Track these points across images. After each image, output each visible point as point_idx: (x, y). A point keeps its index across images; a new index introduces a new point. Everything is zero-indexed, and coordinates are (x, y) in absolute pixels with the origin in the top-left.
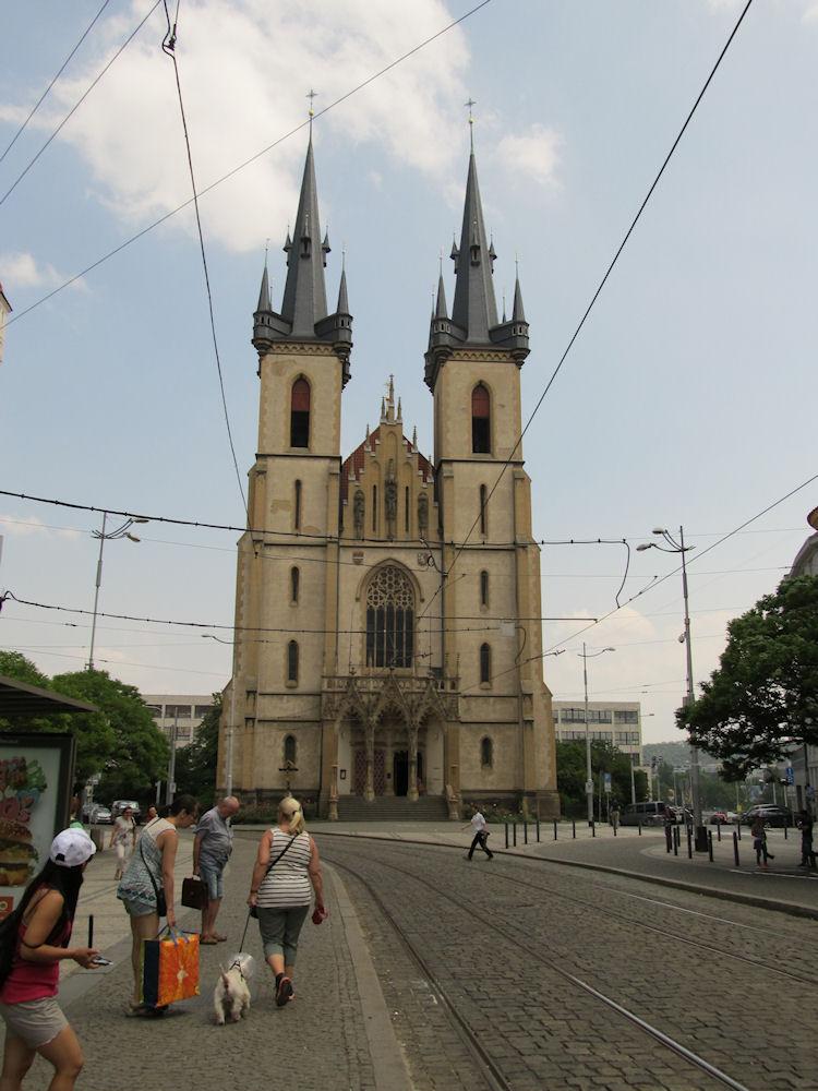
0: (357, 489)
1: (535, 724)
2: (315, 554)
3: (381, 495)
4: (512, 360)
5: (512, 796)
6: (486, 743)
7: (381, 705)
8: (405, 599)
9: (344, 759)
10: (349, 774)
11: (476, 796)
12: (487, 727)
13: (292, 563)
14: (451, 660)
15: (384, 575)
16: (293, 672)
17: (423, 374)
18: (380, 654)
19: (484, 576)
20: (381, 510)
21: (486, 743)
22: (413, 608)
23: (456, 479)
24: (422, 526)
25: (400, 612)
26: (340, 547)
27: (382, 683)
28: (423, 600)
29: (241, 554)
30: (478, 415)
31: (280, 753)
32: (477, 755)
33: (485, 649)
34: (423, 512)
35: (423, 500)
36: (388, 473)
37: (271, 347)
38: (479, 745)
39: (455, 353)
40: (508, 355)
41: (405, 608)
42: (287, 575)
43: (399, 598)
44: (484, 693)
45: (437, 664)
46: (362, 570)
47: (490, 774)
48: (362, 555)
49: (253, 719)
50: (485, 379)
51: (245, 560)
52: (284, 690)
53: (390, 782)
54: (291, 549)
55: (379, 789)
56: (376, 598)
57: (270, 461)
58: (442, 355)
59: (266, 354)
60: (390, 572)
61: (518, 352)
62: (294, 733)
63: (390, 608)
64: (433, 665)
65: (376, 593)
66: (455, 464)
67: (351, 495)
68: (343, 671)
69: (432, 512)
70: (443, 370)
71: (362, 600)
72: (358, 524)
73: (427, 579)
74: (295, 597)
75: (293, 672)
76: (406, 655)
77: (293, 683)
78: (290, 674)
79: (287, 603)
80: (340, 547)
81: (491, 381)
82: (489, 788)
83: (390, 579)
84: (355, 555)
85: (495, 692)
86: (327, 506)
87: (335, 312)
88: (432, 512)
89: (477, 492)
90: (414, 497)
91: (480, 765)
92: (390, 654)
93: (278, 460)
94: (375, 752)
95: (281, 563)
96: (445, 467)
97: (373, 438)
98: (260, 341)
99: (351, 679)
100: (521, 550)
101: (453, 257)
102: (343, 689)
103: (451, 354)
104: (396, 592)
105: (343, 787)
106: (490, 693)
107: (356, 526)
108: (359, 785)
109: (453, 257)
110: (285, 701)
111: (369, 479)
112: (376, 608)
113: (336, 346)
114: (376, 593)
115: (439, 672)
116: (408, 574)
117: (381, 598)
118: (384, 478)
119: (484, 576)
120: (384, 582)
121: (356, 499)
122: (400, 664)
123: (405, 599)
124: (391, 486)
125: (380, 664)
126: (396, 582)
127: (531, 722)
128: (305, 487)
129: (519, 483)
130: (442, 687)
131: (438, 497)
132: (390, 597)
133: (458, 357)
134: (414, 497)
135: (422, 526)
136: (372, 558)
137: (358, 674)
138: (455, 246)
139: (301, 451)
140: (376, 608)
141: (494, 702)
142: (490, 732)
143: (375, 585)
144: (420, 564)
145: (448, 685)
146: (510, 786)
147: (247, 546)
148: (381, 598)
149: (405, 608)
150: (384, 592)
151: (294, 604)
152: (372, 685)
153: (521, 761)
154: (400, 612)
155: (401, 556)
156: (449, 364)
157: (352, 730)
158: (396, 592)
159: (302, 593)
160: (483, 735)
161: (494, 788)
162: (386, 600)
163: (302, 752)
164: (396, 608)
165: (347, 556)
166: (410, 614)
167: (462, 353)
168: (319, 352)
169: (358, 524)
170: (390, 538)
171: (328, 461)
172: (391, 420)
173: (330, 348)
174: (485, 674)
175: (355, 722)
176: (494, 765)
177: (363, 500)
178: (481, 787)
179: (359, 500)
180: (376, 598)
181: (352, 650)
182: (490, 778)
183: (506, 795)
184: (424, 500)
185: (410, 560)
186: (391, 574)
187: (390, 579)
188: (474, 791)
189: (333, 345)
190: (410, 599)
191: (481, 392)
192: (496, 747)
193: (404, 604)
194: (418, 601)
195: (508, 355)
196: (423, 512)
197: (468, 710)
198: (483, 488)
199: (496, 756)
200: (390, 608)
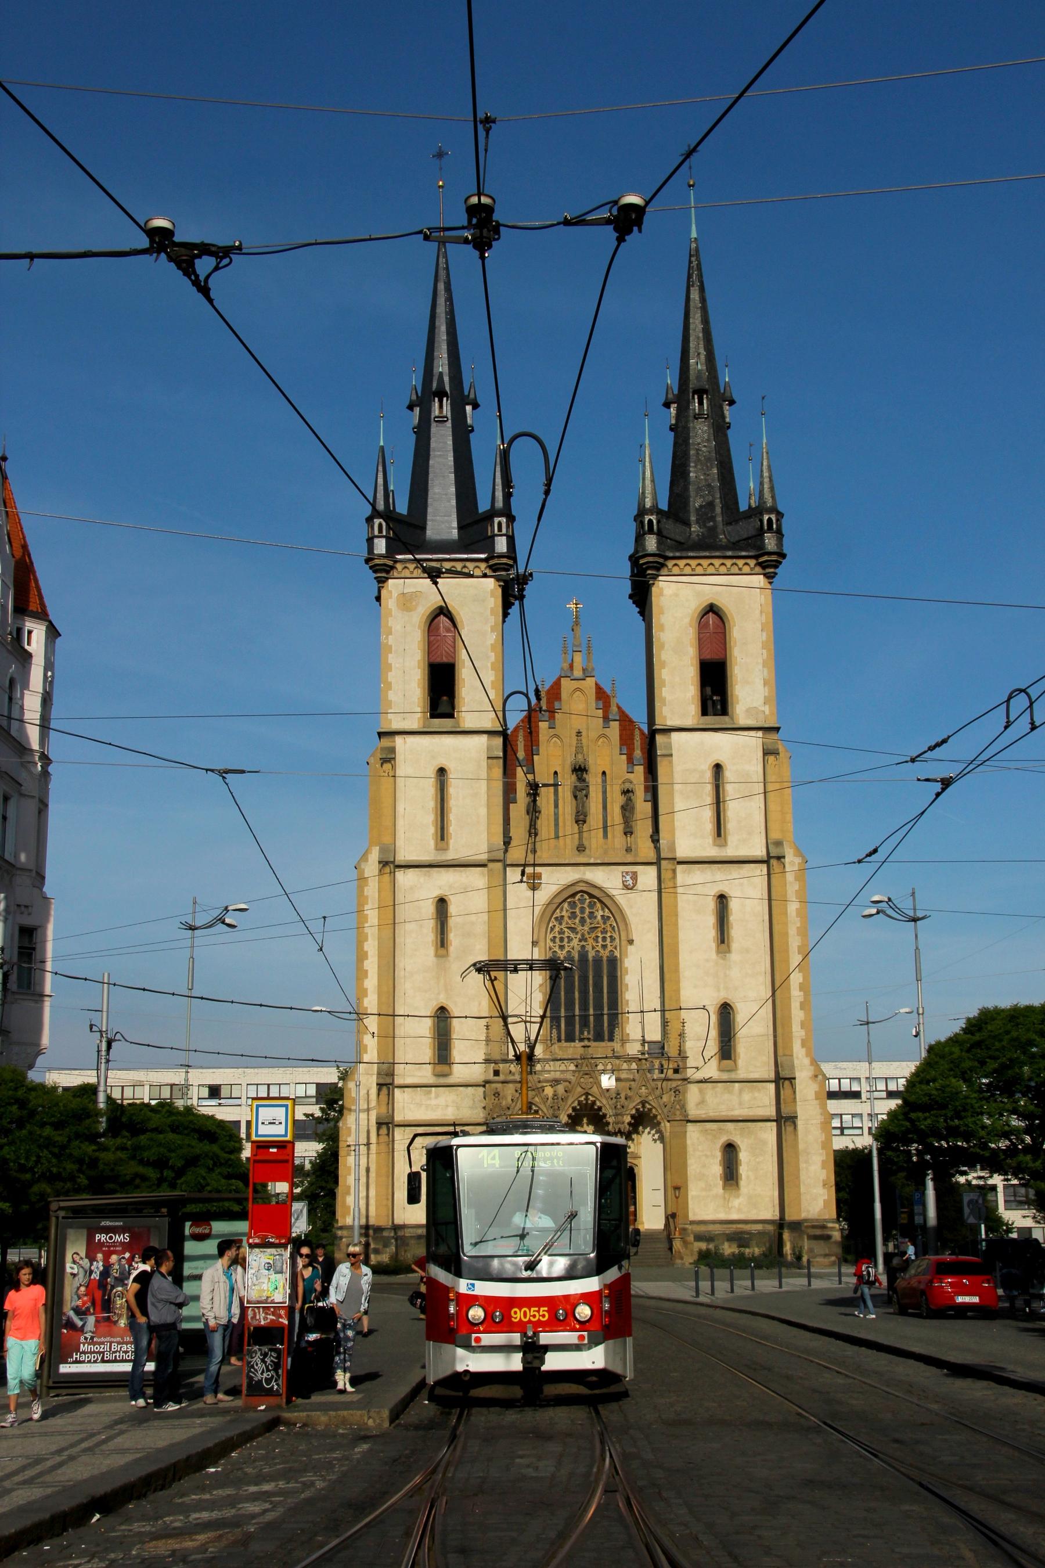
4: (758, 569)
5: (770, 1228)
6: (730, 1150)
8: (604, 939)
11: (717, 1229)
13: (437, 893)
14: (674, 1029)
15: (573, 905)
19: (722, 899)
21: (730, 1150)
22: (617, 953)
23: (674, 757)
25: (598, 961)
26: (506, 866)
27: (572, 1067)
28: (631, 942)
30: (708, 656)
32: (716, 1169)
34: (627, 809)
38: (719, 1155)
39: (670, 563)
41: (605, 954)
43: (596, 939)
44: (725, 1076)
45: (654, 1034)
47: (738, 1196)
50: (715, 602)
52: (432, 1080)
56: (562, 940)
57: (399, 740)
59: (387, 579)
60: (582, 901)
61: (765, 558)
63: (583, 955)
66: (675, 736)
69: (643, 808)
70: (654, 589)
71: (542, 944)
72: (533, 831)
74: (442, 941)
77: (444, 1068)
78: (439, 1056)
79: (431, 951)
80: (506, 866)
82: (734, 1216)
85: (741, 1074)
87: (488, 507)
88: (643, 808)
89: (708, 776)
92: (585, 1023)
93: (411, 739)
96: (660, 739)
98: (377, 562)
102: (517, 1077)
103: (667, 566)
104: (593, 929)
106: (733, 1076)
110: (433, 1095)
114: (561, 932)
117: (570, 939)
118: (570, 760)
120: (573, 915)
122: (599, 1037)
123: (604, 939)
124: (580, 770)
125: (570, 1038)
126: (592, 915)
129: (771, 759)
132: (583, 939)
133: (676, 570)
136: (554, 881)
139: (438, 723)
141: (741, 1091)
143: (559, 920)
149: (605, 954)
150: (573, 929)
151: (442, 951)
154: (598, 961)
155: (600, 877)
158: (593, 929)
160: (723, 1139)
162: (575, 942)
164: (591, 954)
166: (613, 963)
167: (682, 563)
174: (726, 1050)
176: (743, 1183)
178: (722, 1216)
180: (562, 940)
182: (736, 1202)
183: (759, 1227)
184: (628, 791)
185: (607, 879)
187: (582, 910)
188: (714, 1222)
192: (743, 1156)
194: (624, 943)
196: (627, 809)
197: (702, 1102)
198: (718, 768)
199: (743, 1170)
200: (583, 955)
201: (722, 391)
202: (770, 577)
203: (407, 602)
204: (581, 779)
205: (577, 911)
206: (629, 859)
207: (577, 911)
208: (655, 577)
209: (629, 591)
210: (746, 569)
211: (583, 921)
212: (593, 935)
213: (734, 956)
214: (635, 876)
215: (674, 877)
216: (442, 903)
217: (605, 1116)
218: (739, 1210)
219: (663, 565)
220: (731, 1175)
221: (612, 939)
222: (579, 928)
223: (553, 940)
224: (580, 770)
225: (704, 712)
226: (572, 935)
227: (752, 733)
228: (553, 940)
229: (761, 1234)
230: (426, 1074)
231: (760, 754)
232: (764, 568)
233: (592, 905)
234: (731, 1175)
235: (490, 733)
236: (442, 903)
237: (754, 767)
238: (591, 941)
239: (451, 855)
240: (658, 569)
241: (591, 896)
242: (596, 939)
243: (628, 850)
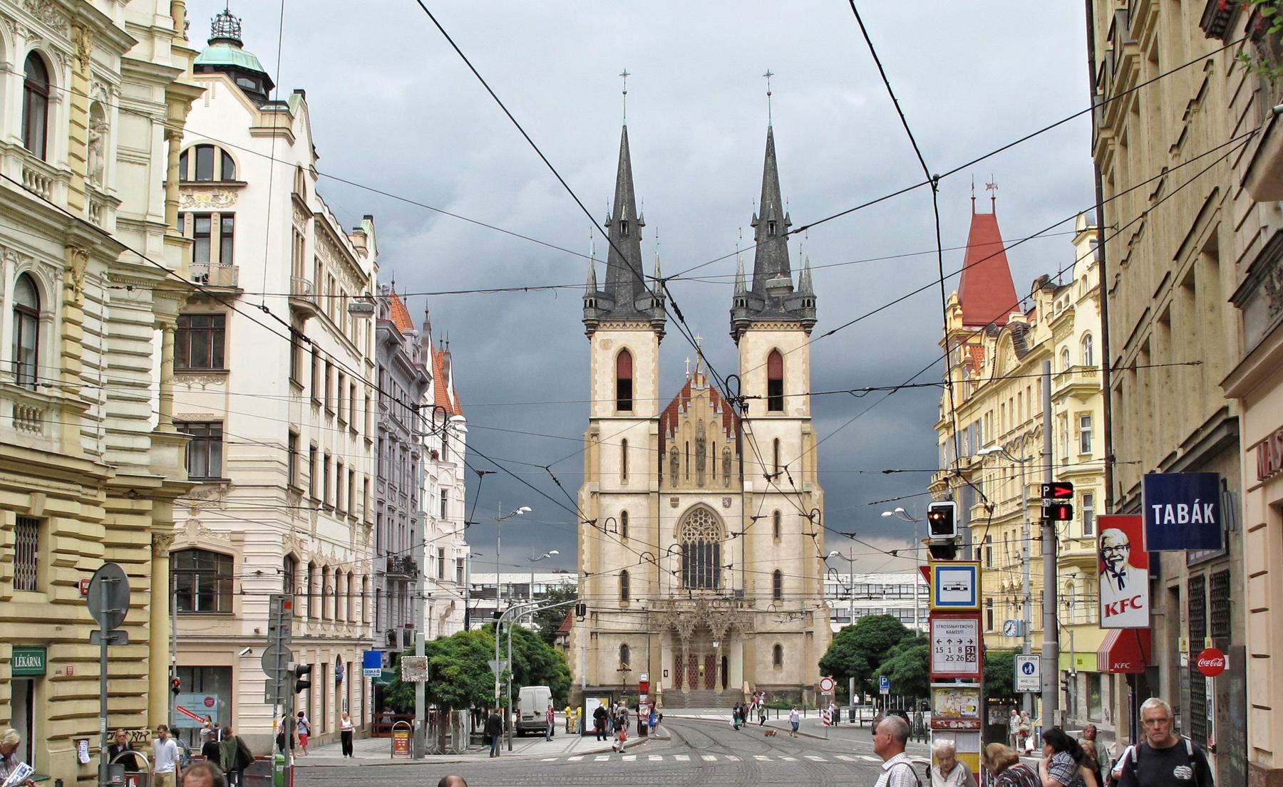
0: (673, 445)
1: (814, 634)
2: (641, 501)
3: (692, 450)
4: (802, 328)
5: (798, 689)
6: (778, 649)
7: (694, 621)
9: (667, 662)
10: (670, 674)
12: (778, 636)
14: (749, 586)
15: (696, 515)
16: (625, 595)
18: (693, 578)
19: (777, 515)
20: (693, 461)
21: (778, 649)
24: (727, 475)
25: (709, 546)
27: (695, 604)
30: (773, 377)
31: (617, 657)
32: (770, 658)
33: (777, 575)
36: (697, 432)
37: (598, 325)
38: (772, 651)
40: (798, 325)
42: (618, 516)
45: (738, 587)
48: (678, 500)
49: (596, 633)
53: (702, 679)
55: (693, 684)
58: (742, 327)
60: (701, 514)
63: (701, 542)
64: (735, 588)
65: (689, 530)
67: (668, 449)
71: (679, 536)
73: (731, 518)
75: (625, 595)
76: (713, 580)
77: (625, 603)
81: (783, 349)
82: (779, 683)
83: (701, 519)
84: (671, 500)
86: (649, 461)
89: (771, 445)
90: (719, 454)
94: (690, 656)
99: (671, 602)
100: (806, 495)
105: (666, 684)
107: (673, 476)
108: (678, 681)
112: (689, 542)
113: (653, 323)
114: (689, 530)
115: (739, 594)
116: (716, 515)
117: (694, 534)
119: (777, 515)
120: (696, 521)
121: (672, 454)
123: (713, 534)
124: (701, 443)
126: (706, 521)
127: (811, 633)
128: (630, 444)
129: (806, 437)
130: (742, 607)
131: (739, 449)
132: (701, 534)
133: (755, 328)
134: (719, 454)
135: (727, 475)
136: (685, 503)
137: (676, 597)
138: (754, 215)
140: (689, 542)
143: (689, 524)
144: (725, 506)
145: (745, 605)
146: (796, 682)
150: (695, 529)
152: (686, 606)
154: (709, 546)
155: (710, 501)
156: (748, 334)
157: (672, 639)
159: (631, 533)
161: (783, 683)
162: (697, 535)
163: (633, 656)
165: (666, 501)
166: (717, 547)
167: (759, 324)
168: (638, 328)
169: (674, 475)
171: (648, 422)
173: (648, 325)
174: (777, 594)
175: (674, 633)
176: (784, 665)
177: (678, 454)
179: (675, 456)
180: (689, 534)
182: (780, 676)
183: (793, 688)
185: (716, 503)
186: (700, 513)
187: (701, 519)
188: (768, 685)
189: (650, 322)
190: (717, 534)
192: (785, 651)
193: (713, 539)
195: (798, 325)
196: (727, 463)
199: (784, 659)
200: (701, 542)
202: (809, 333)
203: (606, 345)
204: (702, 447)
205: (698, 519)
206: (727, 491)
207: (698, 519)
208: (744, 332)
210: (795, 328)
211: (701, 524)
212: (706, 532)
213: (783, 545)
214: (730, 501)
215: (751, 502)
216: (624, 514)
217: (711, 630)
218: (782, 679)
219: (749, 325)
220: (778, 660)
221: (717, 534)
222: (699, 528)
223: (685, 534)
224: (701, 443)
225: (770, 409)
226: (695, 532)
229: (794, 692)
230: (616, 605)
231: (800, 434)
232: (805, 328)
234: (778, 660)
235: (652, 420)
236: (624, 514)
237: (796, 440)
238: (705, 535)
239: (630, 488)
240: (746, 328)
241: (706, 511)
242: (708, 534)
243: (727, 486)
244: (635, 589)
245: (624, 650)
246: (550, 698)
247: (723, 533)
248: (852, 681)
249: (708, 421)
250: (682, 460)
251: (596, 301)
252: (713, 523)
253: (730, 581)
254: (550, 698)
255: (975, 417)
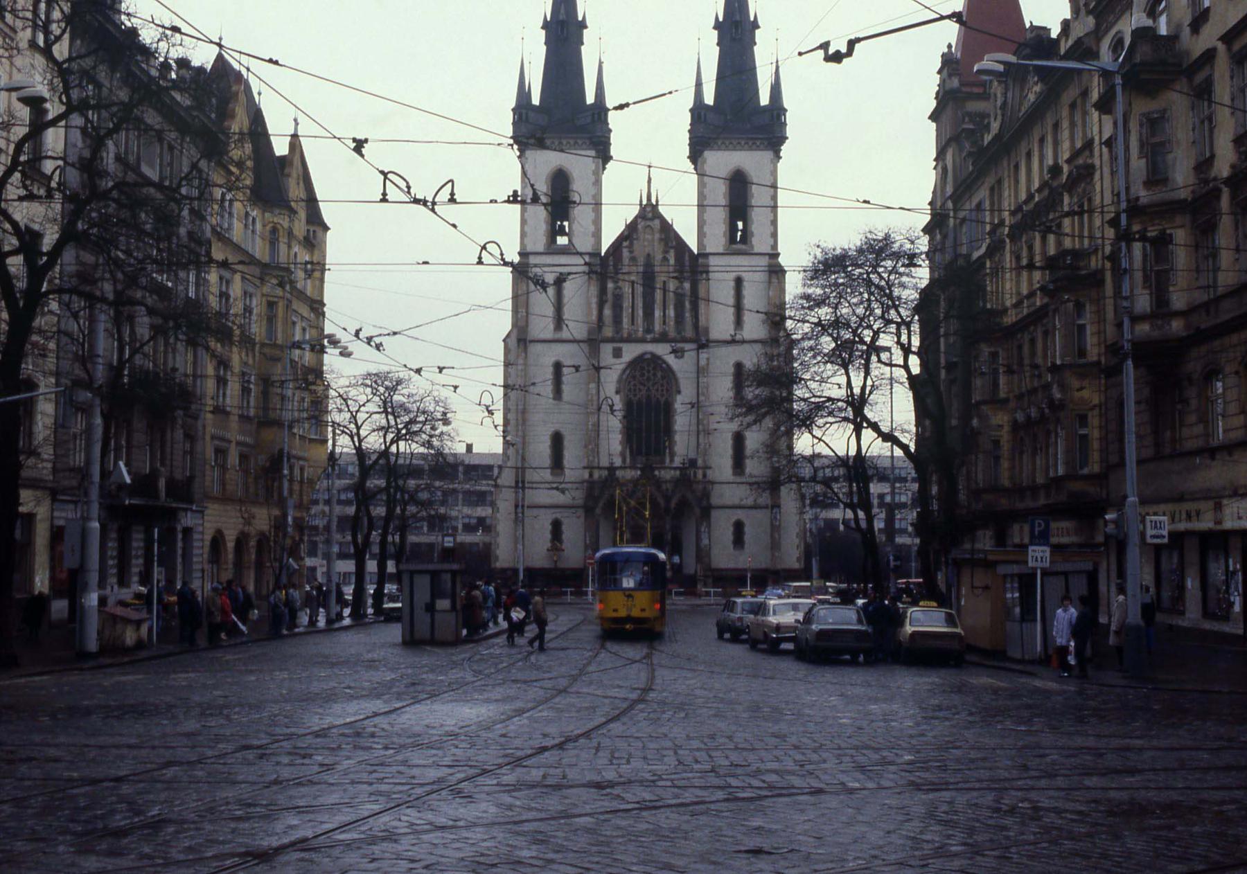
6: (739, 527)
13: (553, 360)
15: (642, 368)
17: (686, 151)
28: (679, 392)
29: (507, 351)
35: (679, 298)
38: (731, 529)
41: (662, 400)
43: (657, 390)
45: (692, 455)
46: (619, 365)
51: (512, 358)
54: (553, 345)
62: (558, 516)
68: (605, 462)
72: (617, 320)
83: (649, 372)
91: (732, 546)
95: (545, 357)
97: (632, 228)
99: (612, 469)
101: (715, 28)
104: (654, 385)
109: (715, 28)
111: (632, 273)
112: (635, 400)
114: (635, 385)
115: (693, 463)
117: (640, 390)
120: (643, 375)
124: (649, 278)
126: (655, 375)
132: (648, 389)
136: (631, 352)
140: (635, 400)
142: (740, 515)
147: (513, 342)
148: (640, 390)
149: (662, 400)
150: (641, 384)
153: (775, 545)
155: (662, 350)
160: (733, 520)
162: (644, 392)
169: (617, 320)
170: (649, 330)
172: (649, 213)
176: (746, 546)
179: (618, 298)
181: (613, 444)
187: (649, 372)
190: (667, 390)
191: (739, 184)
192: (747, 529)
193: (662, 395)
199: (747, 538)
201: (752, 19)
209: (688, 154)
210: (762, 147)
212: (656, 387)
224: (649, 278)
226: (642, 387)
227: (761, 257)
228: (630, 390)
233: (654, 368)
234: (739, 540)
239: (565, 334)
244: (572, 456)
245: (557, 527)
246: (469, 447)
247: (674, 388)
248: (828, 584)
249: (659, 257)
250: (627, 304)
251: (527, 114)
252: (663, 378)
253: (682, 445)
254: (469, 447)
255: (975, 201)
